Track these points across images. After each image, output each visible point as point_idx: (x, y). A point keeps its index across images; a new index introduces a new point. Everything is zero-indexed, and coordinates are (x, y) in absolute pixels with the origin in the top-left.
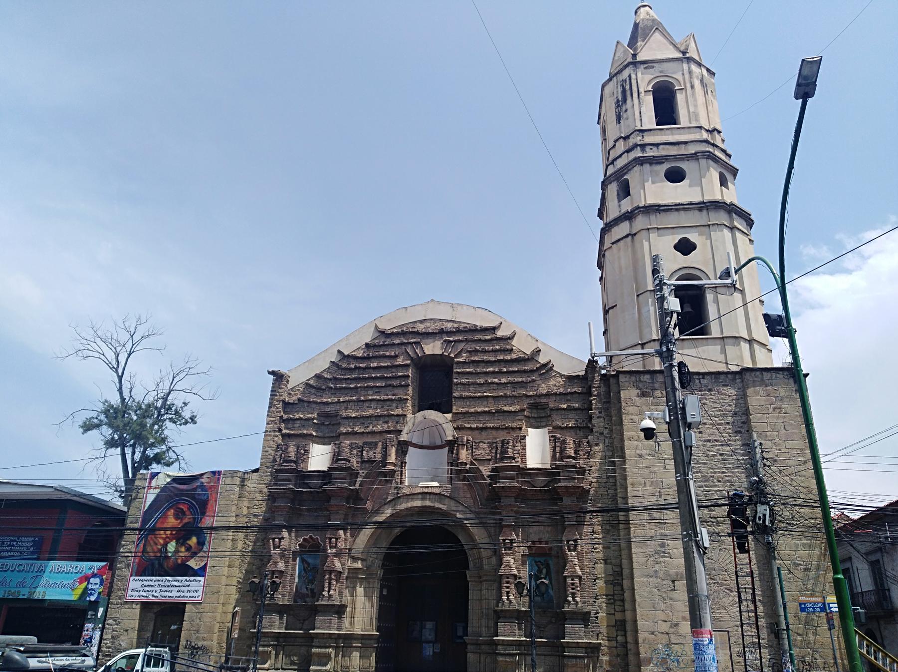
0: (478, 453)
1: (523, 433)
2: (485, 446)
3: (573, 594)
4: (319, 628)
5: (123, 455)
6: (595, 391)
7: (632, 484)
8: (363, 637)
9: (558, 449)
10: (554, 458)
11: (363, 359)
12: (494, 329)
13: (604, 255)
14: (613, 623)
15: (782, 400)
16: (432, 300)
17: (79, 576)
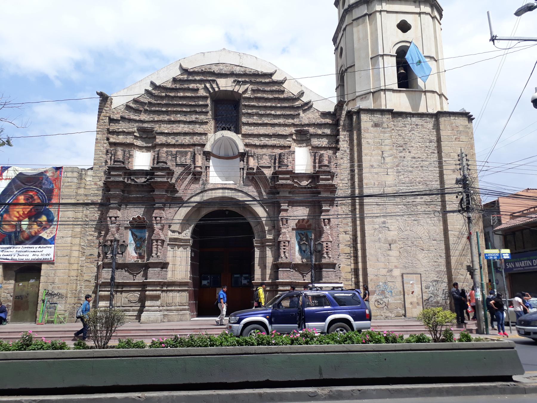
1: (291, 149)
2: (267, 157)
3: (327, 252)
4: (150, 278)
6: (342, 123)
7: (366, 184)
8: (181, 284)
9: (317, 161)
10: (314, 167)
12: (271, 75)
14: (350, 270)
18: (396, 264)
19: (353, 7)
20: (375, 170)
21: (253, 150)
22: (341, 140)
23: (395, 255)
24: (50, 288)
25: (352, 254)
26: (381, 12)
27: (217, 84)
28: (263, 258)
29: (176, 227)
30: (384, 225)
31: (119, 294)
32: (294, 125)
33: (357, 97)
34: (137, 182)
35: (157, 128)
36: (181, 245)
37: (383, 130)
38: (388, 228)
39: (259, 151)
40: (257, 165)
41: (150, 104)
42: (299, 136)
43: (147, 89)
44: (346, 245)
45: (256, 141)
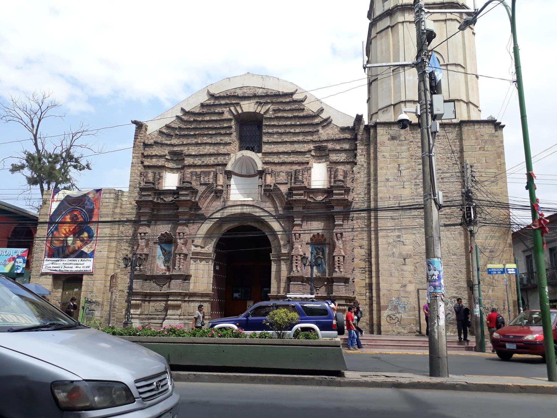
0: (279, 179)
2: (284, 174)
3: (339, 267)
4: (172, 289)
5: (42, 187)
6: (359, 137)
8: (203, 295)
9: (332, 176)
10: (330, 182)
11: (199, 114)
12: (292, 94)
13: (371, 42)
14: (364, 285)
15: (486, 142)
16: (248, 73)
17: (8, 257)
18: (411, 279)
19: (377, 20)
20: (390, 184)
21: (273, 168)
22: (358, 154)
23: (409, 270)
24: (89, 296)
25: (367, 269)
26: (403, 22)
27: (241, 107)
28: (279, 271)
29: (198, 242)
30: (399, 239)
31: (147, 303)
32: (312, 141)
33: (379, 110)
34: (165, 201)
35: (185, 150)
36: (204, 259)
37: (400, 143)
38: (403, 242)
39: (278, 168)
40: (274, 182)
41: (180, 128)
42: (318, 152)
43: (178, 115)
44: (361, 260)
45: (276, 159)
